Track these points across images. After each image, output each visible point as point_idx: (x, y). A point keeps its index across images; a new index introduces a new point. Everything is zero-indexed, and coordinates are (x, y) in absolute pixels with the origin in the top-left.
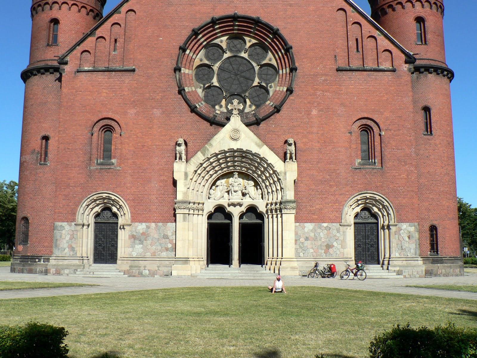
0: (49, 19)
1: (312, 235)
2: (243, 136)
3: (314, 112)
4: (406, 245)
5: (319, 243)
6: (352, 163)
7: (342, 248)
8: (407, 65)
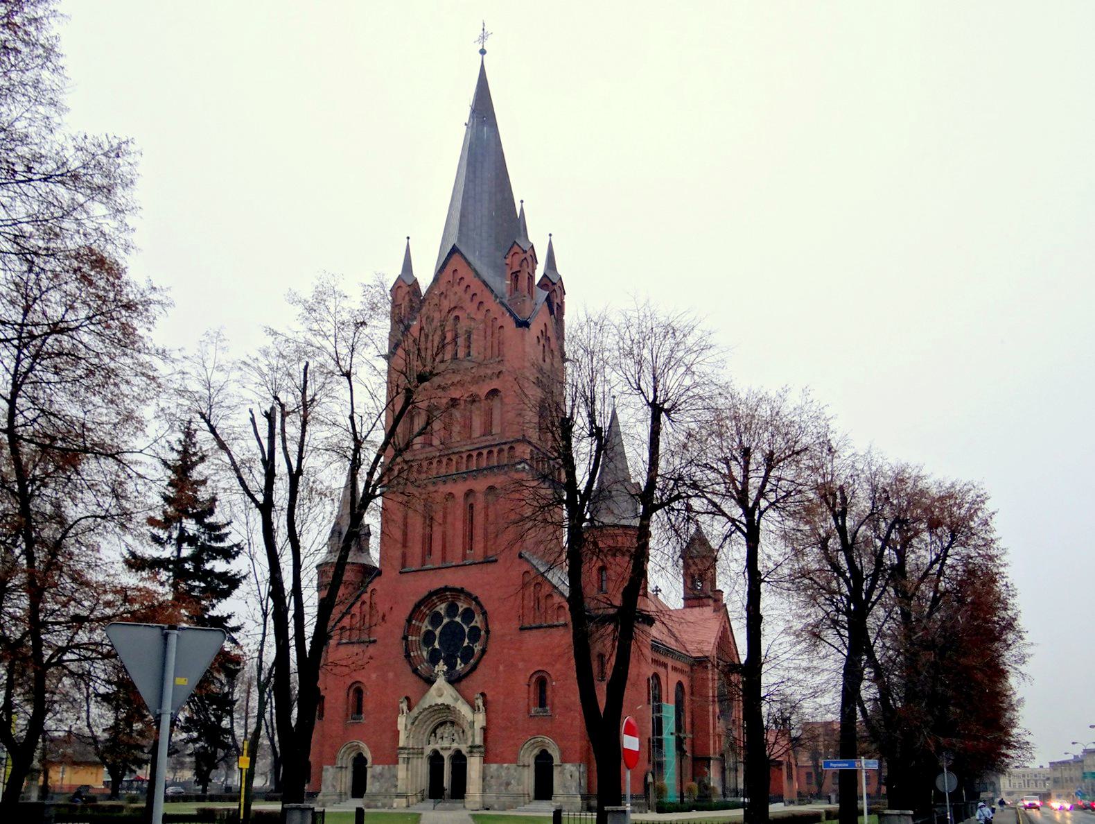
1: (496, 773)
3: (501, 668)
4: (568, 784)
6: (529, 712)
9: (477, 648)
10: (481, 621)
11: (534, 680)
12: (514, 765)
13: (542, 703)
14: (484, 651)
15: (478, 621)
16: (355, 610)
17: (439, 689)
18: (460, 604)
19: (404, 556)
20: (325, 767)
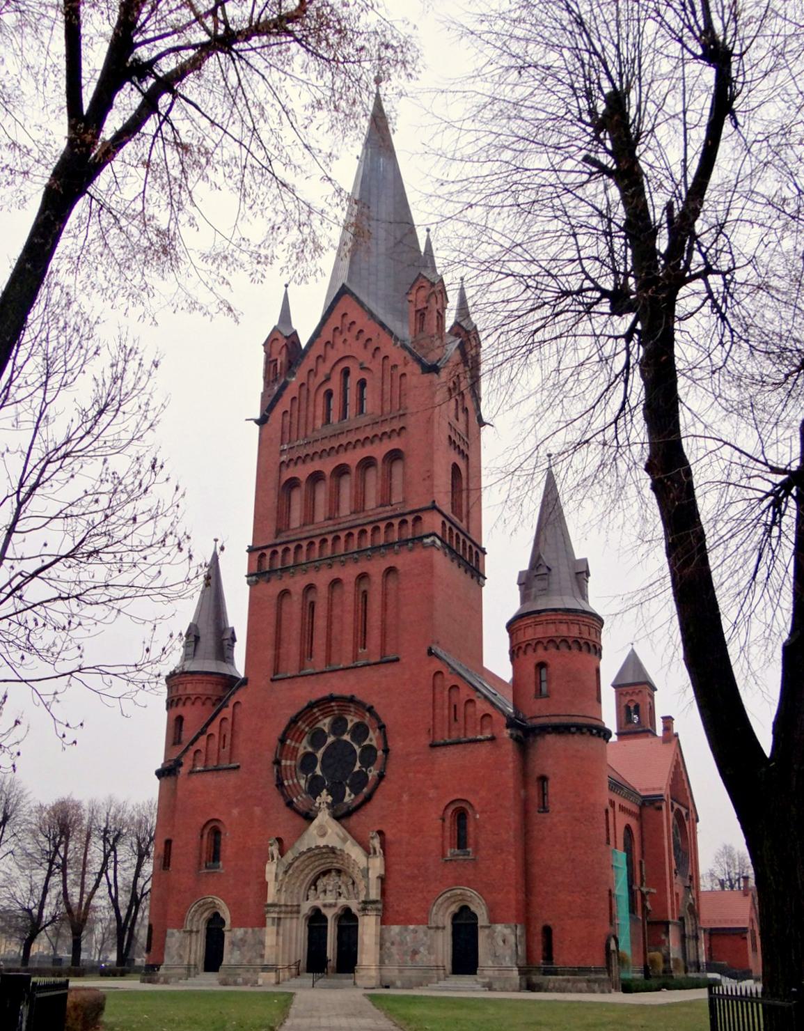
1: (398, 938)
2: (330, 831)
3: (405, 798)
5: (405, 948)
6: (444, 855)
7: (429, 953)
8: (509, 731)
9: (373, 773)
10: (377, 739)
11: (449, 812)
12: (422, 928)
13: (462, 843)
14: (381, 777)
15: (373, 738)
16: (214, 729)
17: (321, 827)
18: (349, 718)
19: (277, 658)
20: (169, 931)
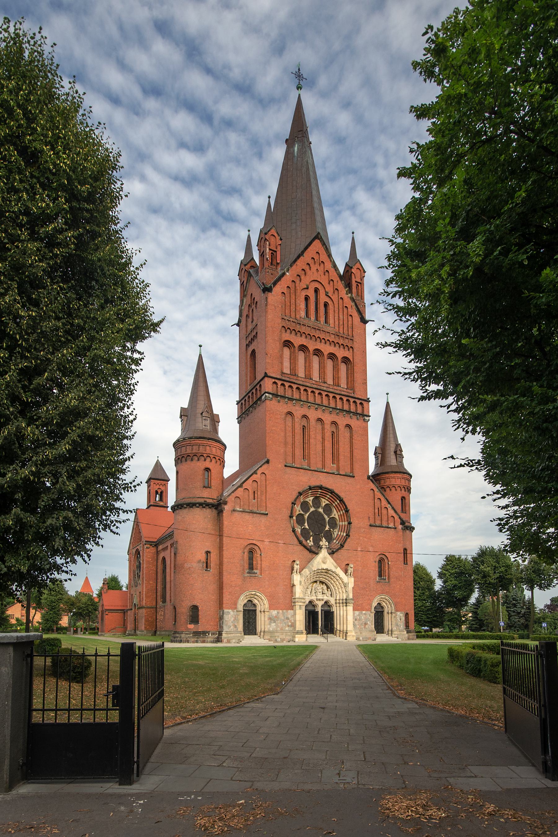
0: (203, 468)
2: (328, 561)
4: (399, 623)
20: (226, 611)
